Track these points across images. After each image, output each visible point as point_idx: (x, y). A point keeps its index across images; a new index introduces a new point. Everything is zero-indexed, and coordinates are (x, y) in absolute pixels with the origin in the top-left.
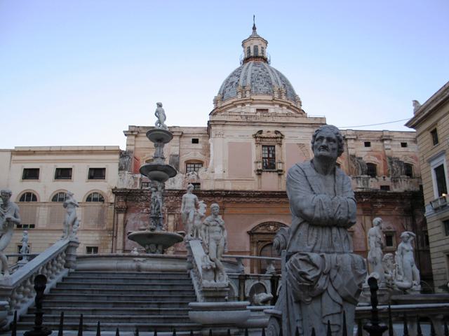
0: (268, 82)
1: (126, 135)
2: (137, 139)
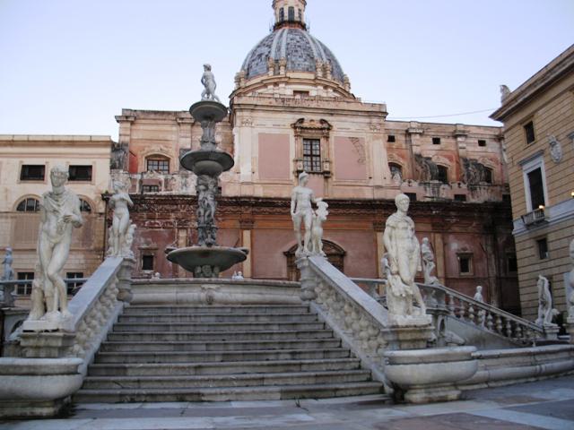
0: (309, 55)
1: (118, 121)
2: (134, 127)
